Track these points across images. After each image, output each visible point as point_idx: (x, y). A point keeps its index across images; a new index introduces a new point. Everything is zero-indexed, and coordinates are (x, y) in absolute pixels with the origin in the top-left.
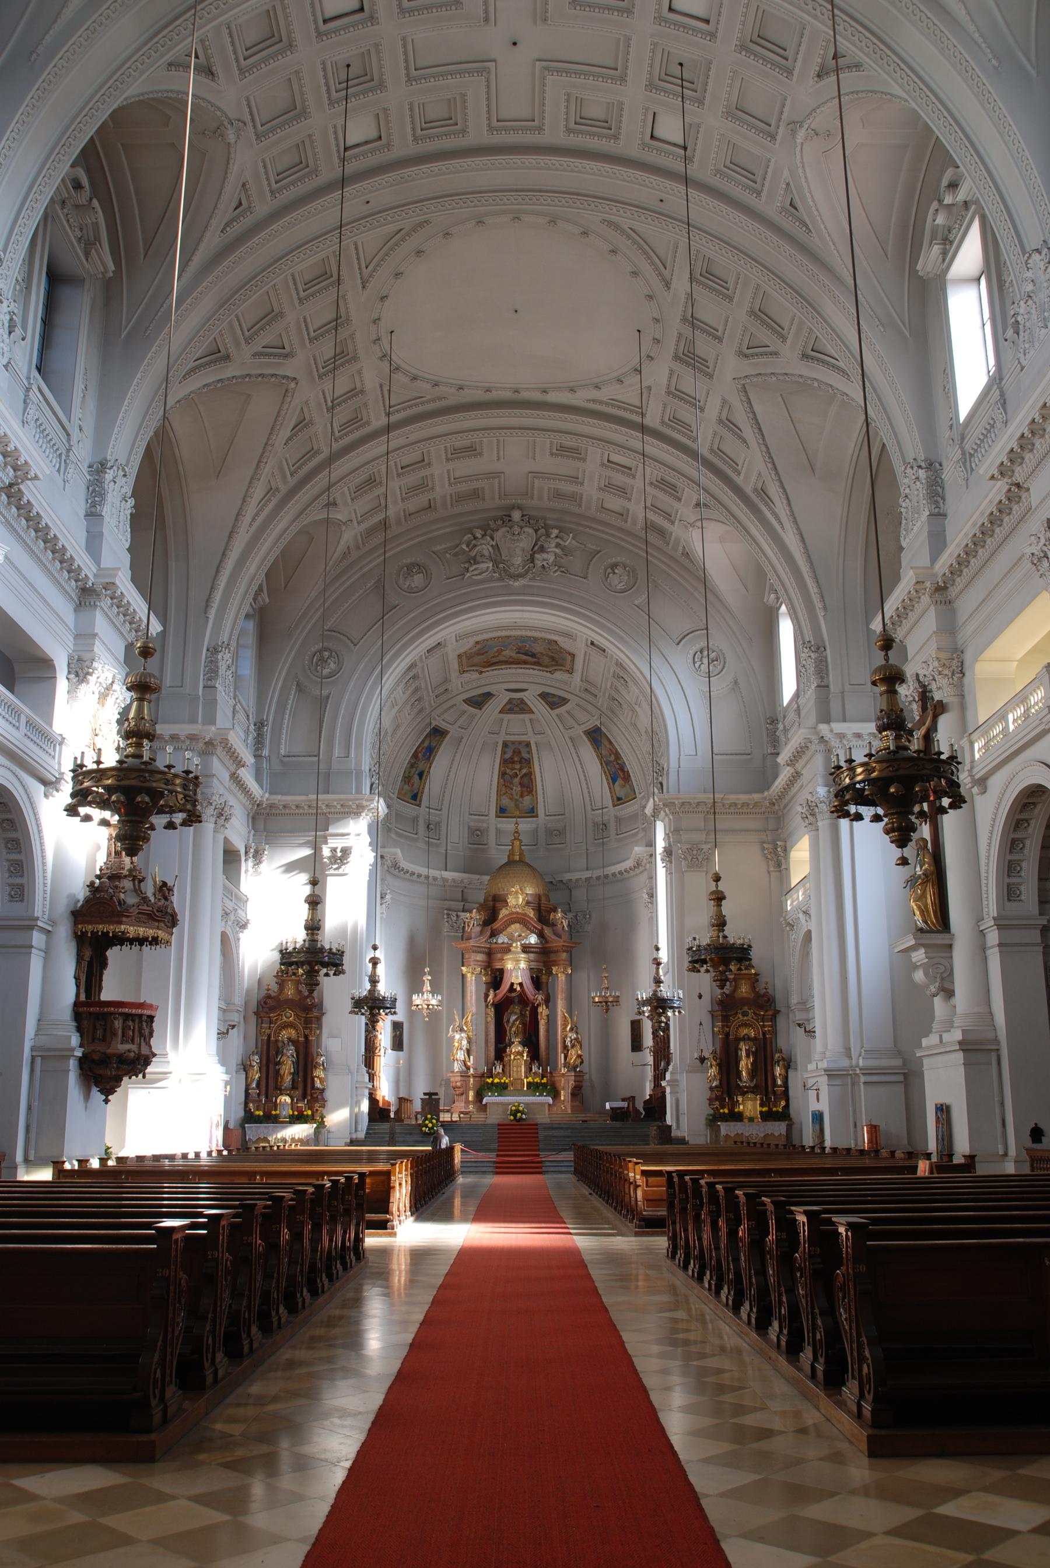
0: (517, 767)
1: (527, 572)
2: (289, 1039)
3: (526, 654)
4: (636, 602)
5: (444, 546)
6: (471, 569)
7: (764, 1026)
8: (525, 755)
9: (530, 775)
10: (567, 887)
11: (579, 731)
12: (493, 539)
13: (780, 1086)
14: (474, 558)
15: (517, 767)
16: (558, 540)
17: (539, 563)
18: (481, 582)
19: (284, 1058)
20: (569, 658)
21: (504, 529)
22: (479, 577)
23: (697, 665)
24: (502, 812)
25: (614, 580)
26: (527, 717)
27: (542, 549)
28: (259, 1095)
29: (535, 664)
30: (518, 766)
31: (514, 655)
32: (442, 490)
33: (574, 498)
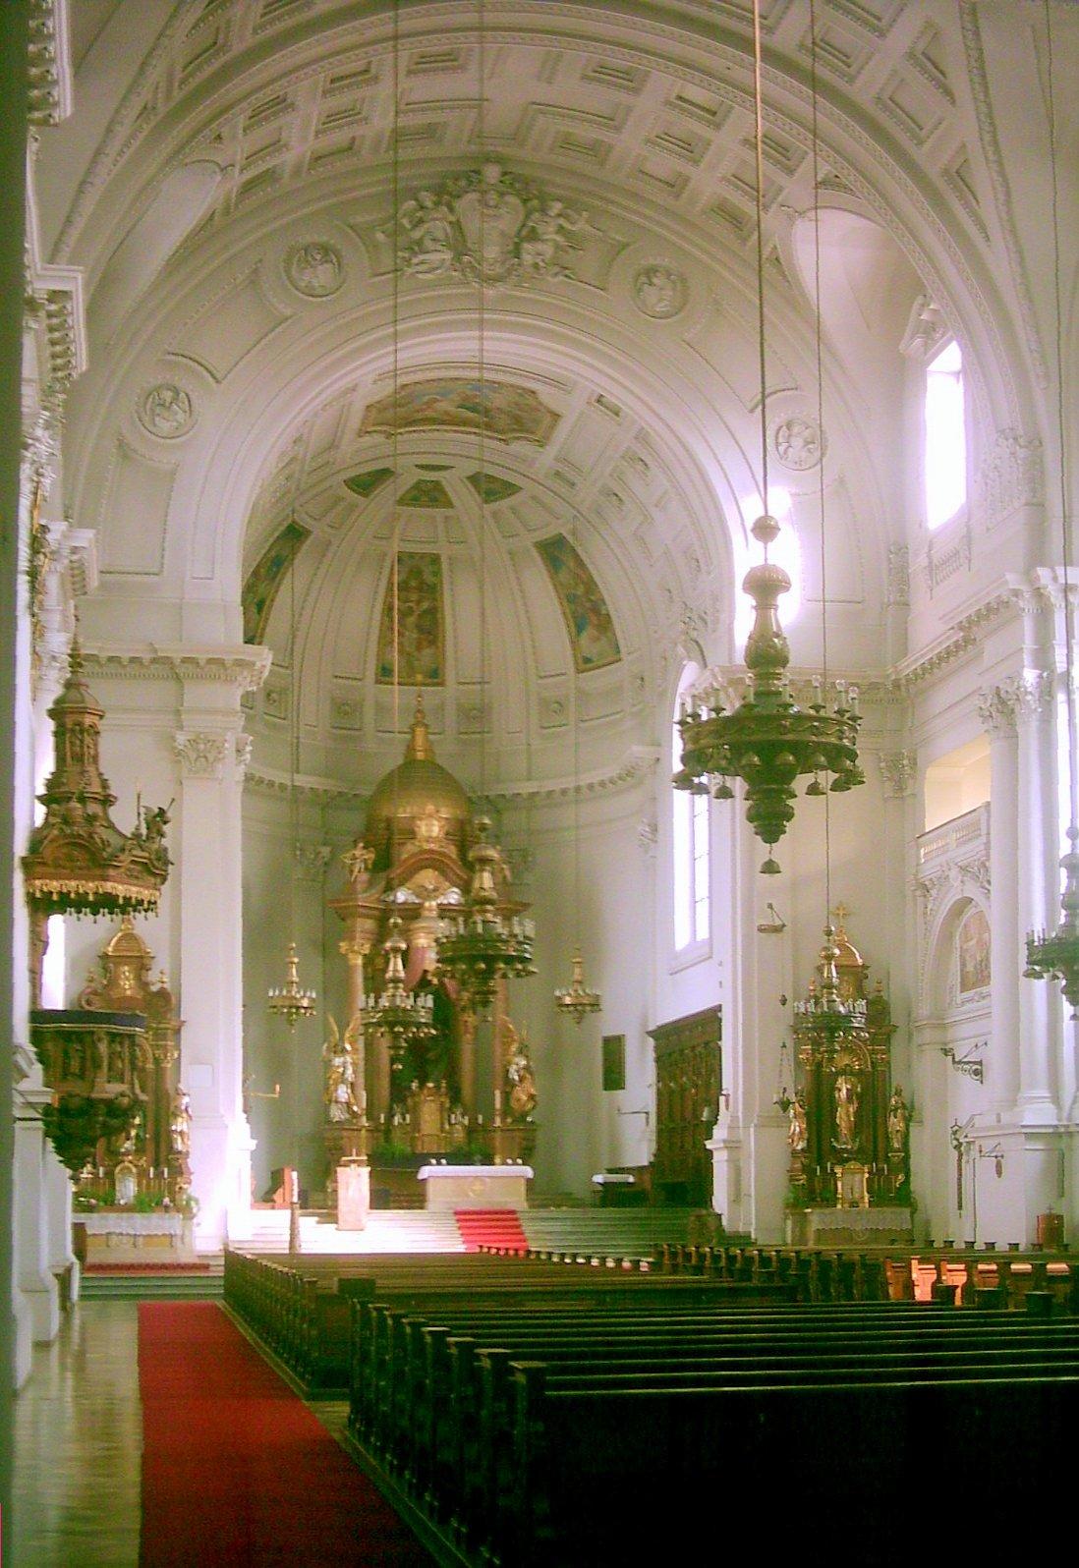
1: (509, 272)
4: (686, 336)
5: (368, 218)
6: (415, 261)
7: (873, 1052)
8: (429, 579)
10: (495, 805)
11: (528, 541)
12: (451, 210)
13: (899, 1150)
14: (419, 242)
16: (561, 221)
17: (528, 259)
18: (427, 286)
20: (547, 420)
21: (473, 196)
22: (430, 276)
23: (782, 449)
24: (385, 673)
25: (651, 295)
26: (439, 513)
27: (533, 236)
29: (488, 427)
30: (414, 597)
31: (452, 409)
32: (381, 121)
33: (597, 151)
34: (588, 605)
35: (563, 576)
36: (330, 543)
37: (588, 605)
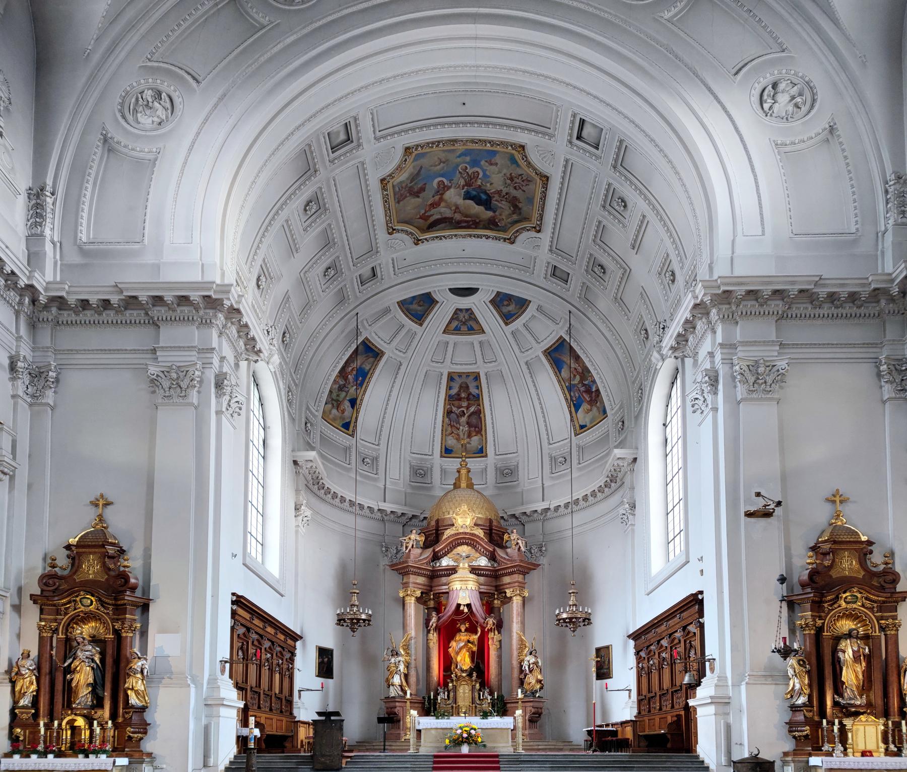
0: (464, 405)
3: (479, 202)
8: (473, 391)
9: (478, 413)
11: (538, 351)
15: (464, 405)
24: (447, 452)
26: (475, 338)
29: (492, 224)
30: (465, 404)
31: (460, 201)
34: (582, 389)
35: (565, 373)
36: (401, 364)
37: (582, 389)
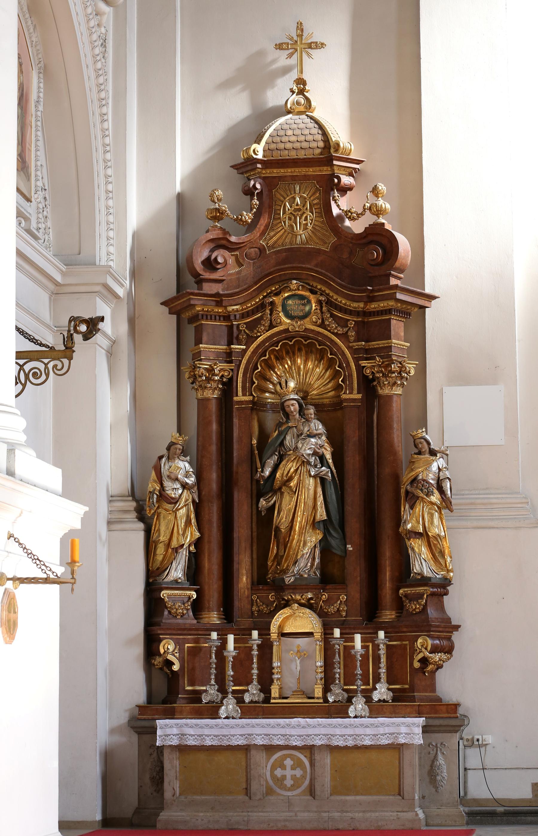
2: (304, 393)
19: (289, 466)
28: (197, 607)
